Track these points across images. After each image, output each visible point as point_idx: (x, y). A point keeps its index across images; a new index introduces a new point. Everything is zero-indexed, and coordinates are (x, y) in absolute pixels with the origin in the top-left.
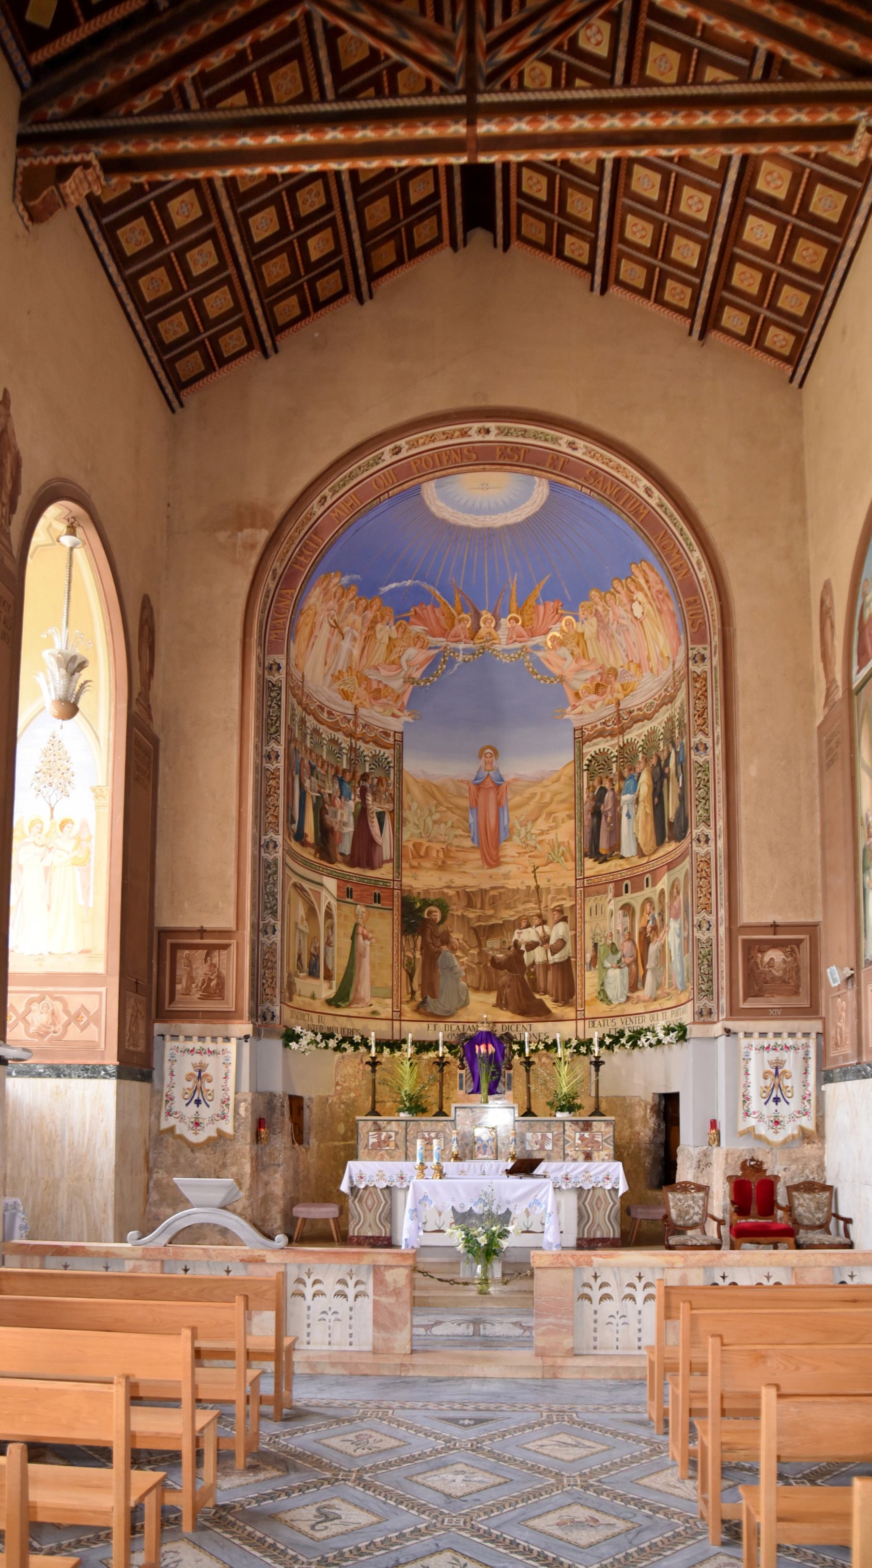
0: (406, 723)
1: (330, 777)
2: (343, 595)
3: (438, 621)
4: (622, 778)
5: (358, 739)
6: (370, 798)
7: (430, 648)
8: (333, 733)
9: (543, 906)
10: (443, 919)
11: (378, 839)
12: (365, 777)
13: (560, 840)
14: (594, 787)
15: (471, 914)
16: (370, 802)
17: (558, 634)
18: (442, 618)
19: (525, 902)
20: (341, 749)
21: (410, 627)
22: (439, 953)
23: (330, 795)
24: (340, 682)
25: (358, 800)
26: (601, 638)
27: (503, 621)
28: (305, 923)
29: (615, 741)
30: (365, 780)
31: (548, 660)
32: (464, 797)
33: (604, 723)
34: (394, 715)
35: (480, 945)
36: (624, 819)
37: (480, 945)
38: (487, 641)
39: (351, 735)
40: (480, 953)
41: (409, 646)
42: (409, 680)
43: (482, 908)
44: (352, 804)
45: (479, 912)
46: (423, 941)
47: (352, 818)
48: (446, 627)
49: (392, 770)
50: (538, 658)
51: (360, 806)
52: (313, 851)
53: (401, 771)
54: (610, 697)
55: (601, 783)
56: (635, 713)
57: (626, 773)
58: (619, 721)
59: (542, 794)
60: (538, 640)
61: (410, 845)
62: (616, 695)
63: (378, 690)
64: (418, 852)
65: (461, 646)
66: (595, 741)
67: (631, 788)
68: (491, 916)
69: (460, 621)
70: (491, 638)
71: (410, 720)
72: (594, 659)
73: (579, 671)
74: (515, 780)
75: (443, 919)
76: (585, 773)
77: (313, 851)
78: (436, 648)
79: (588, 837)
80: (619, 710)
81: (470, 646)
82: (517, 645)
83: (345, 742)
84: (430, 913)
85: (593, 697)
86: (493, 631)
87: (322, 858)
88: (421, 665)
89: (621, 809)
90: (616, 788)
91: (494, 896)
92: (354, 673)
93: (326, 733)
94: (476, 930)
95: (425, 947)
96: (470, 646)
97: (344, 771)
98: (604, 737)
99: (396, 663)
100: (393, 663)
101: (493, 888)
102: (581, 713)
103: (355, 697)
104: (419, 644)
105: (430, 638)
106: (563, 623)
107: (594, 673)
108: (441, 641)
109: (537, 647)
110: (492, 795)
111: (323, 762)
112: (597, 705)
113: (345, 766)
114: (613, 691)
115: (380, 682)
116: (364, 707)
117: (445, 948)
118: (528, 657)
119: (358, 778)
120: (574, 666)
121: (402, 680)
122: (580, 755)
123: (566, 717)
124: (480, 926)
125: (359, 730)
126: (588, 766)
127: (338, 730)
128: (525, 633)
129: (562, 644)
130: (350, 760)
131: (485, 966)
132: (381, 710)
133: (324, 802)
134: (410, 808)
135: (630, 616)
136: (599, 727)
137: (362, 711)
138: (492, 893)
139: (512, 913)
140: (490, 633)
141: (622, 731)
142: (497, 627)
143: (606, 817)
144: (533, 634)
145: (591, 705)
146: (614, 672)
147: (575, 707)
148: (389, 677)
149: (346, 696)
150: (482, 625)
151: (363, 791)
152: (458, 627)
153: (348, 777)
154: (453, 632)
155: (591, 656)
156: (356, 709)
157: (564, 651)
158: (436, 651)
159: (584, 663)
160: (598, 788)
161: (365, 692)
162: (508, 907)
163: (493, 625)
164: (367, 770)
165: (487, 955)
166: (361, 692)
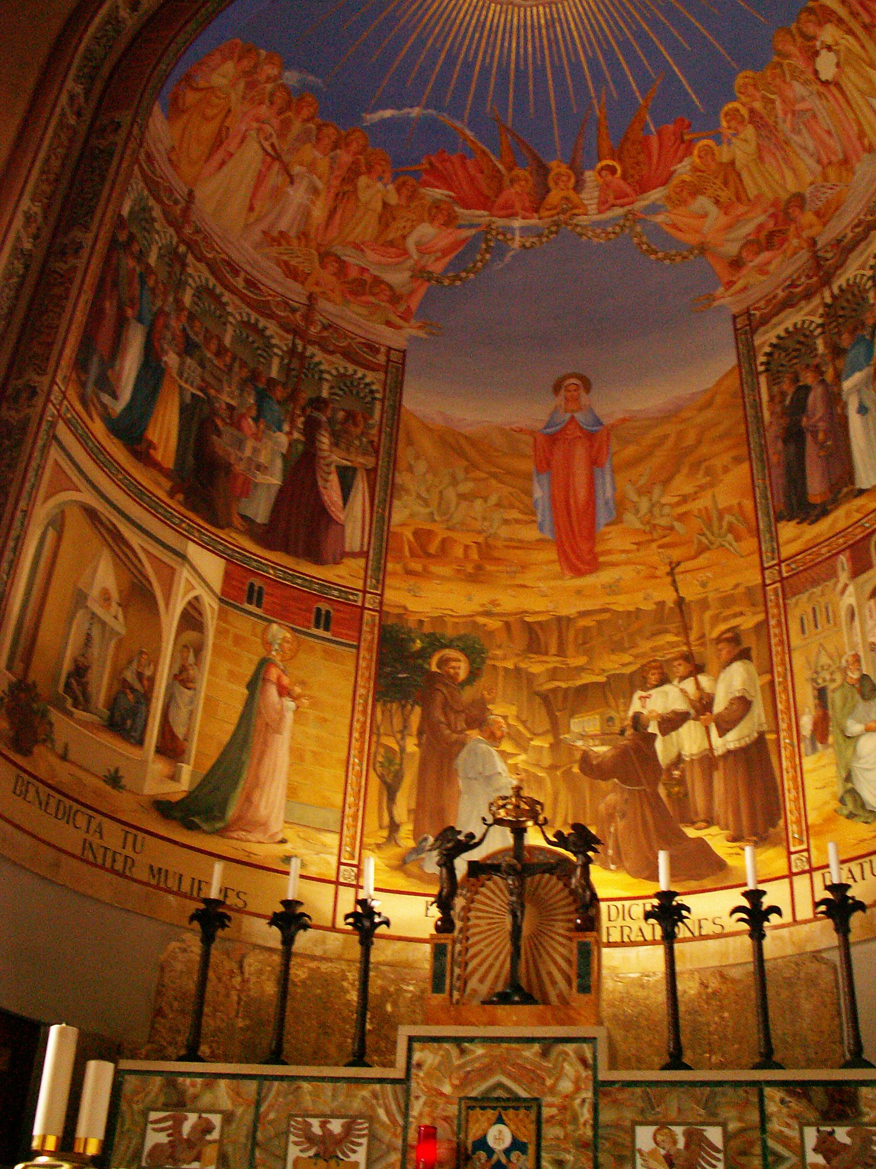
0: (412, 339)
1: (236, 379)
2: (289, 106)
3: (472, 180)
4: (837, 352)
5: (313, 343)
6: (325, 440)
7: (460, 227)
8: (254, 316)
9: (693, 636)
10: (474, 675)
11: (336, 509)
12: (318, 403)
13: (720, 507)
14: (783, 394)
15: (536, 667)
16: (325, 447)
17: (687, 178)
18: (479, 175)
19: (654, 634)
20: (270, 346)
21: (423, 190)
22: (462, 744)
23: (230, 407)
24: (282, 249)
25: (296, 435)
26: (767, 157)
27: (589, 175)
28: (114, 608)
29: (816, 301)
30: (318, 410)
31: (674, 226)
32: (523, 456)
33: (789, 286)
34: (389, 323)
35: (555, 728)
36: (855, 422)
37: (555, 728)
38: (564, 212)
39: (296, 332)
40: (556, 746)
41: (421, 220)
42: (420, 274)
43: (561, 652)
44: (283, 439)
45: (553, 661)
46: (426, 717)
47: (279, 464)
48: (487, 192)
49: (378, 406)
50: (657, 227)
51: (300, 447)
52: (168, 485)
53: (397, 407)
54: (795, 242)
55: (797, 379)
56: (850, 235)
57: (845, 340)
58: (819, 266)
59: (680, 435)
60: (656, 195)
61: (408, 534)
62: (805, 235)
63: (361, 283)
64: (423, 547)
65: (517, 223)
66: (775, 320)
67: (862, 359)
68: (581, 669)
69: (512, 182)
70: (572, 208)
71: (421, 334)
72: (758, 197)
73: (729, 227)
74: (624, 420)
75: (474, 675)
76: (763, 379)
77: (168, 485)
78: (471, 226)
79: (779, 481)
80: (815, 252)
81: (534, 221)
82: (619, 211)
83: (280, 340)
84: (443, 662)
85: (765, 256)
86: (572, 194)
87: (189, 504)
88: (445, 252)
89: (845, 406)
90: (829, 376)
91: (586, 629)
92: (314, 244)
93: (237, 310)
94: (546, 699)
95: (428, 730)
96: (534, 221)
97: (271, 382)
98: (792, 306)
99: (397, 247)
100: (391, 244)
101: (583, 614)
102: (745, 288)
103: (311, 280)
104: (441, 219)
105: (459, 210)
106: (696, 152)
107: (762, 218)
108: (481, 216)
109: (654, 209)
110: (580, 453)
111: (221, 352)
112: (772, 268)
113: (274, 373)
114: (799, 230)
115: (363, 270)
116: (328, 300)
117: (474, 734)
118: (638, 229)
119: (302, 402)
120: (724, 220)
121: (407, 275)
122: (747, 353)
123: (716, 303)
124: (555, 690)
125: (313, 330)
126: (767, 364)
127: (271, 316)
128: (629, 190)
129: (696, 191)
130: (286, 369)
131: (568, 773)
132: (364, 311)
133: (214, 412)
134: (410, 469)
135: (817, 87)
136: (781, 294)
137: (322, 304)
138: (582, 623)
139: (627, 658)
140: (567, 199)
141: (826, 281)
142: (579, 186)
143: (815, 434)
144: (643, 187)
145: (762, 270)
146: (799, 200)
147: (730, 284)
148: (379, 264)
149: (292, 273)
150: (551, 185)
151: (311, 429)
152: (511, 192)
153: (279, 393)
154: (500, 201)
155: (752, 192)
156: (311, 297)
157: (703, 203)
158: (473, 232)
159: (742, 209)
160: (791, 391)
161: (334, 279)
162: (617, 647)
163: (573, 180)
164: (325, 394)
165: (571, 748)
166: (327, 276)
